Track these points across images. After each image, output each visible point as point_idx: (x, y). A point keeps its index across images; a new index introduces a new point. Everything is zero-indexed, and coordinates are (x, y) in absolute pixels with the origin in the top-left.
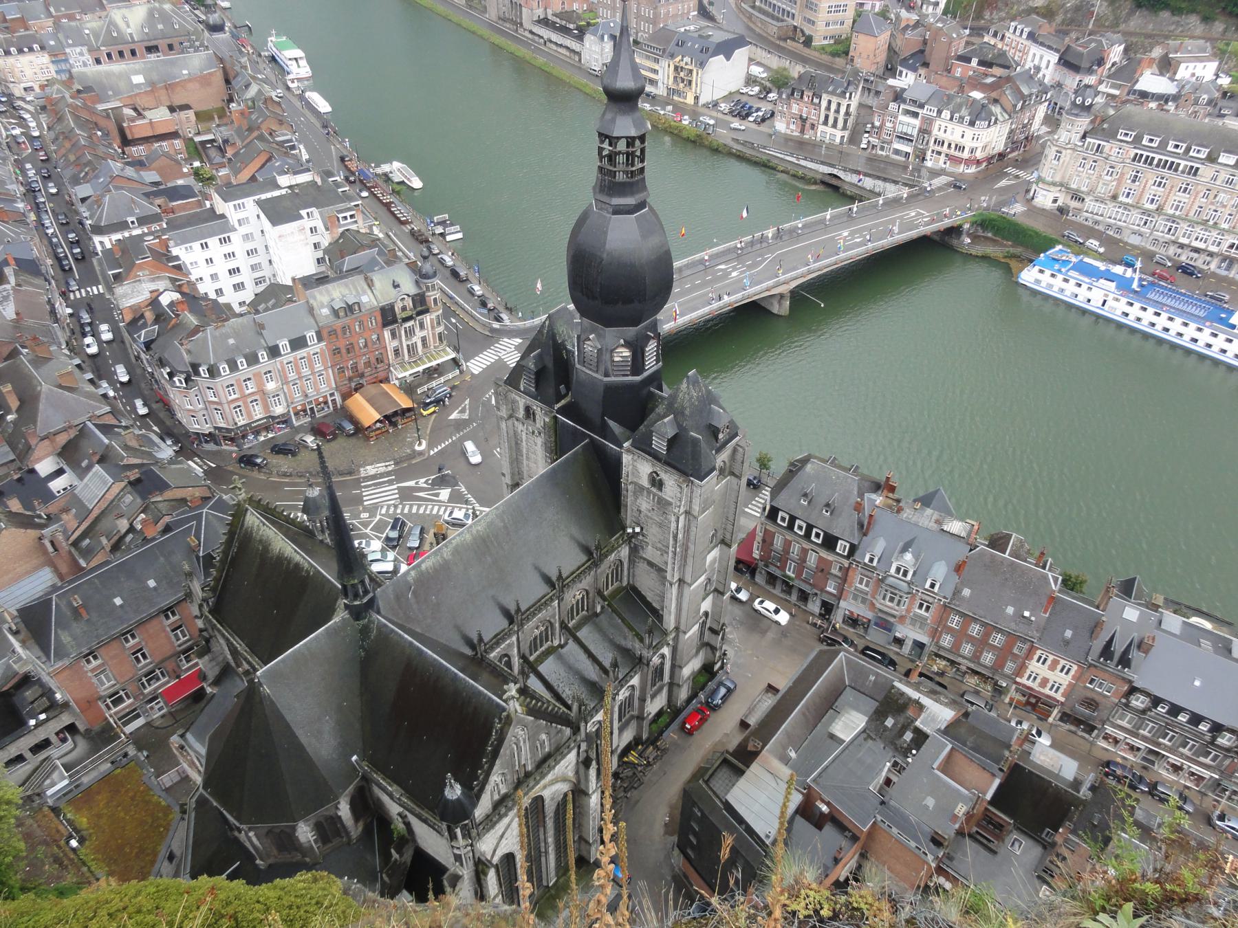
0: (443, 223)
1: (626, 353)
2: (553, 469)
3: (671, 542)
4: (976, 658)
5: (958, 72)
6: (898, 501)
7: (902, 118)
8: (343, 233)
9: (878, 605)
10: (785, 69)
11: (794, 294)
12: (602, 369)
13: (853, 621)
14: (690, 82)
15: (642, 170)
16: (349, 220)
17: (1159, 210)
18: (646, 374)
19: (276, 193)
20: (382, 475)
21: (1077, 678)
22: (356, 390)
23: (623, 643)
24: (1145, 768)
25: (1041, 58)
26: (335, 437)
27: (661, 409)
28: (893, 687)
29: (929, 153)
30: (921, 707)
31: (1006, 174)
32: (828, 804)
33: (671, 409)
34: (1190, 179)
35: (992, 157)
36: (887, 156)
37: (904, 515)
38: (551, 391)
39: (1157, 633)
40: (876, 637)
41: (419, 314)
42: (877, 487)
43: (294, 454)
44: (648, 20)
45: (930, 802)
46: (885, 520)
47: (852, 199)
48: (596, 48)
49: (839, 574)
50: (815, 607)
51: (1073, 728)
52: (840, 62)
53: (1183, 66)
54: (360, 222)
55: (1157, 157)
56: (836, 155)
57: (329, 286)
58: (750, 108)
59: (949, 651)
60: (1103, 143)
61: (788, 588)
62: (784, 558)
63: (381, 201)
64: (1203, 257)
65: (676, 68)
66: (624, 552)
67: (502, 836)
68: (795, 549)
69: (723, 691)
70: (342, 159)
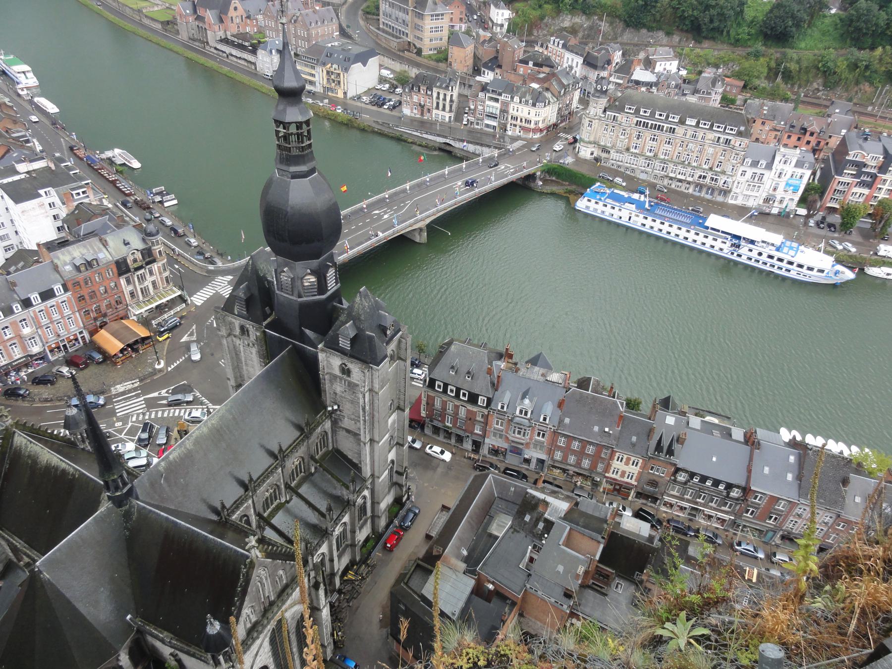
0: (160, 193)
1: (313, 279)
2: (267, 370)
3: (361, 413)
4: (578, 464)
5: (521, 71)
6: (516, 364)
7: (488, 103)
8: (77, 207)
9: (510, 438)
10: (405, 71)
11: (429, 226)
12: (296, 293)
13: (495, 451)
14: (339, 82)
15: (310, 146)
16: (82, 195)
17: (655, 156)
18: (329, 293)
19: (16, 178)
20: (130, 391)
21: (643, 467)
22: (101, 327)
23: (334, 492)
24: (690, 520)
25: (573, 60)
26: (87, 365)
27: (342, 318)
28: (527, 493)
29: (509, 126)
30: (546, 504)
31: (560, 138)
32: (493, 583)
33: (350, 317)
34: (671, 135)
35: (550, 127)
36: (481, 129)
37: (521, 373)
38: (259, 313)
39: (687, 430)
40: (512, 460)
41: (148, 263)
42: (500, 356)
43: (52, 383)
44: (303, 39)
45: (561, 568)
46: (508, 378)
47: (461, 159)
48: (268, 59)
49: (482, 420)
50: (468, 445)
51: (644, 501)
52: (442, 66)
53: (658, 64)
54: (92, 197)
55: (650, 122)
56: (446, 129)
57: (70, 248)
58: (384, 99)
59: (561, 462)
61: (448, 435)
62: (443, 414)
63: (107, 179)
64: (685, 185)
65: (328, 72)
66: (328, 425)
67: (256, 655)
68: (450, 407)
69: (411, 515)
70: (71, 149)
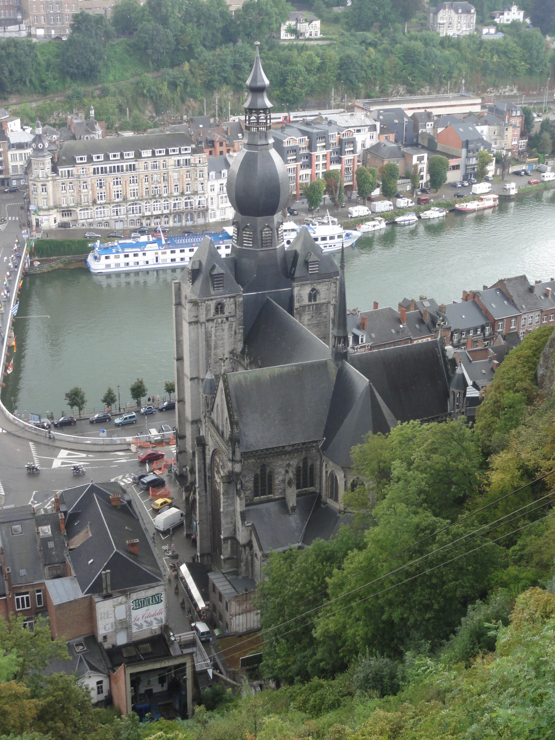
17: (125, 200)
34: (133, 173)
55: (108, 166)
60: (70, 169)
64: (164, 219)
